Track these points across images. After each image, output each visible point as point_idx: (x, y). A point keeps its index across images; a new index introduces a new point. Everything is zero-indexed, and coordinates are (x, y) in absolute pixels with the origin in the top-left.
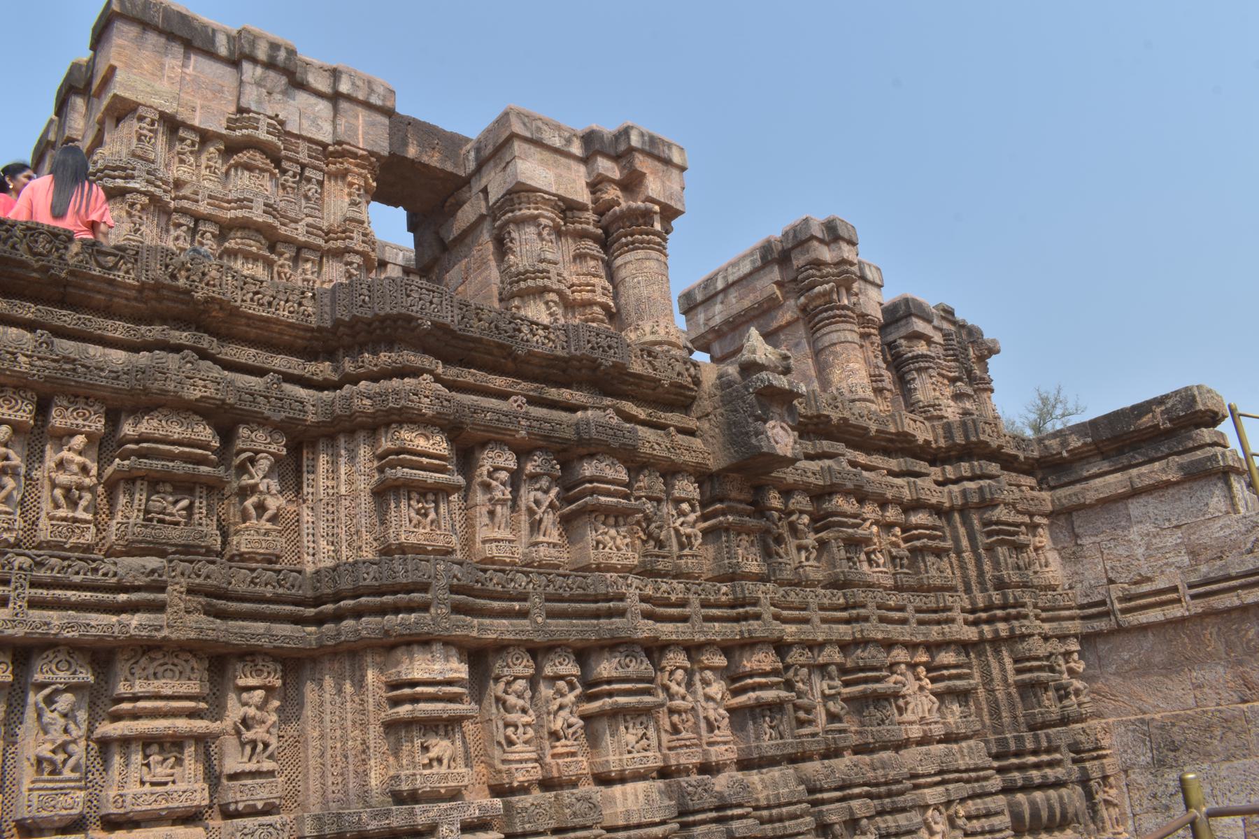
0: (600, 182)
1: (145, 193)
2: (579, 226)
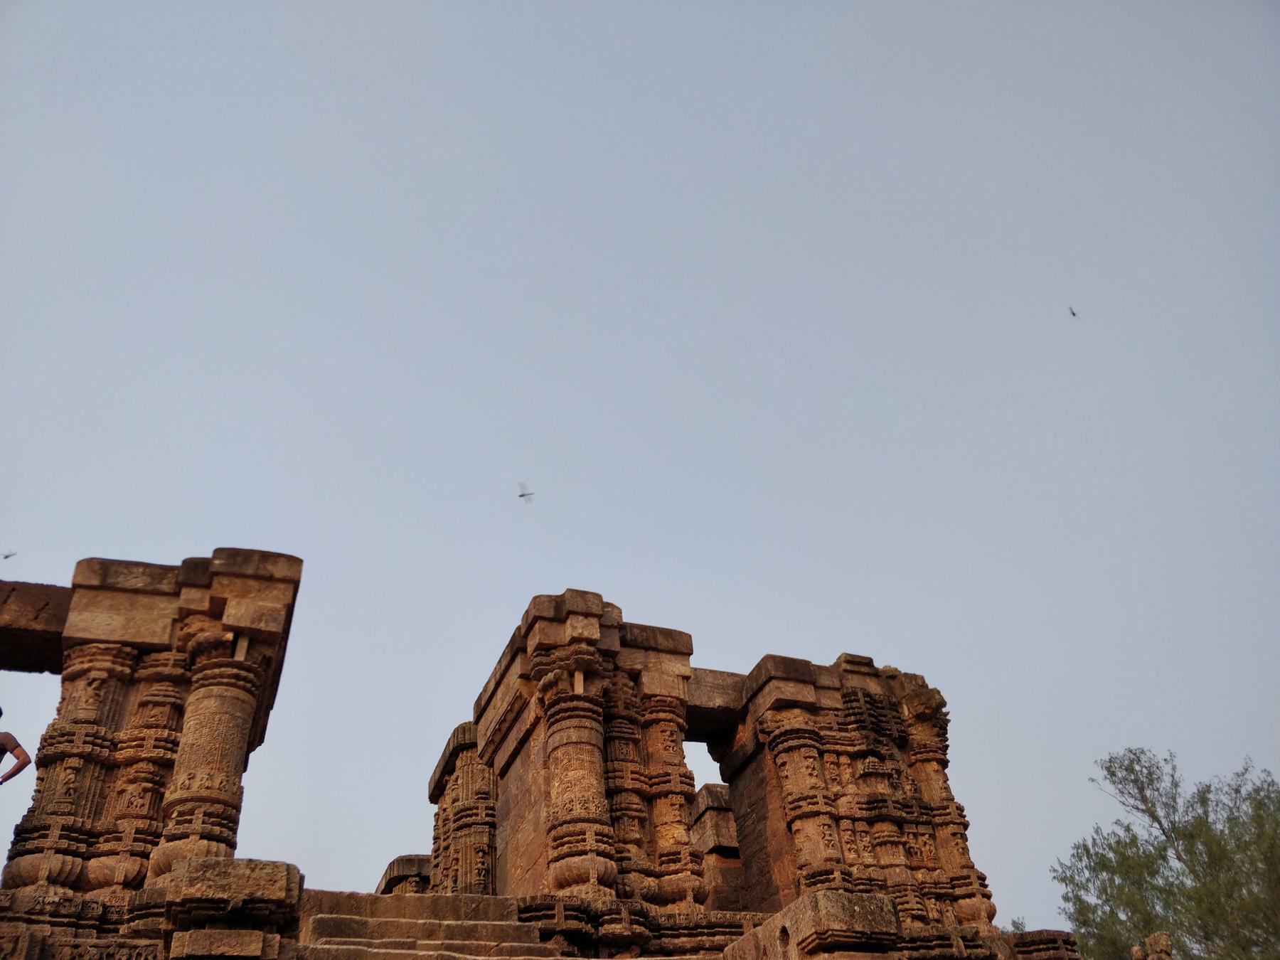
0: (187, 616)
2: (151, 671)
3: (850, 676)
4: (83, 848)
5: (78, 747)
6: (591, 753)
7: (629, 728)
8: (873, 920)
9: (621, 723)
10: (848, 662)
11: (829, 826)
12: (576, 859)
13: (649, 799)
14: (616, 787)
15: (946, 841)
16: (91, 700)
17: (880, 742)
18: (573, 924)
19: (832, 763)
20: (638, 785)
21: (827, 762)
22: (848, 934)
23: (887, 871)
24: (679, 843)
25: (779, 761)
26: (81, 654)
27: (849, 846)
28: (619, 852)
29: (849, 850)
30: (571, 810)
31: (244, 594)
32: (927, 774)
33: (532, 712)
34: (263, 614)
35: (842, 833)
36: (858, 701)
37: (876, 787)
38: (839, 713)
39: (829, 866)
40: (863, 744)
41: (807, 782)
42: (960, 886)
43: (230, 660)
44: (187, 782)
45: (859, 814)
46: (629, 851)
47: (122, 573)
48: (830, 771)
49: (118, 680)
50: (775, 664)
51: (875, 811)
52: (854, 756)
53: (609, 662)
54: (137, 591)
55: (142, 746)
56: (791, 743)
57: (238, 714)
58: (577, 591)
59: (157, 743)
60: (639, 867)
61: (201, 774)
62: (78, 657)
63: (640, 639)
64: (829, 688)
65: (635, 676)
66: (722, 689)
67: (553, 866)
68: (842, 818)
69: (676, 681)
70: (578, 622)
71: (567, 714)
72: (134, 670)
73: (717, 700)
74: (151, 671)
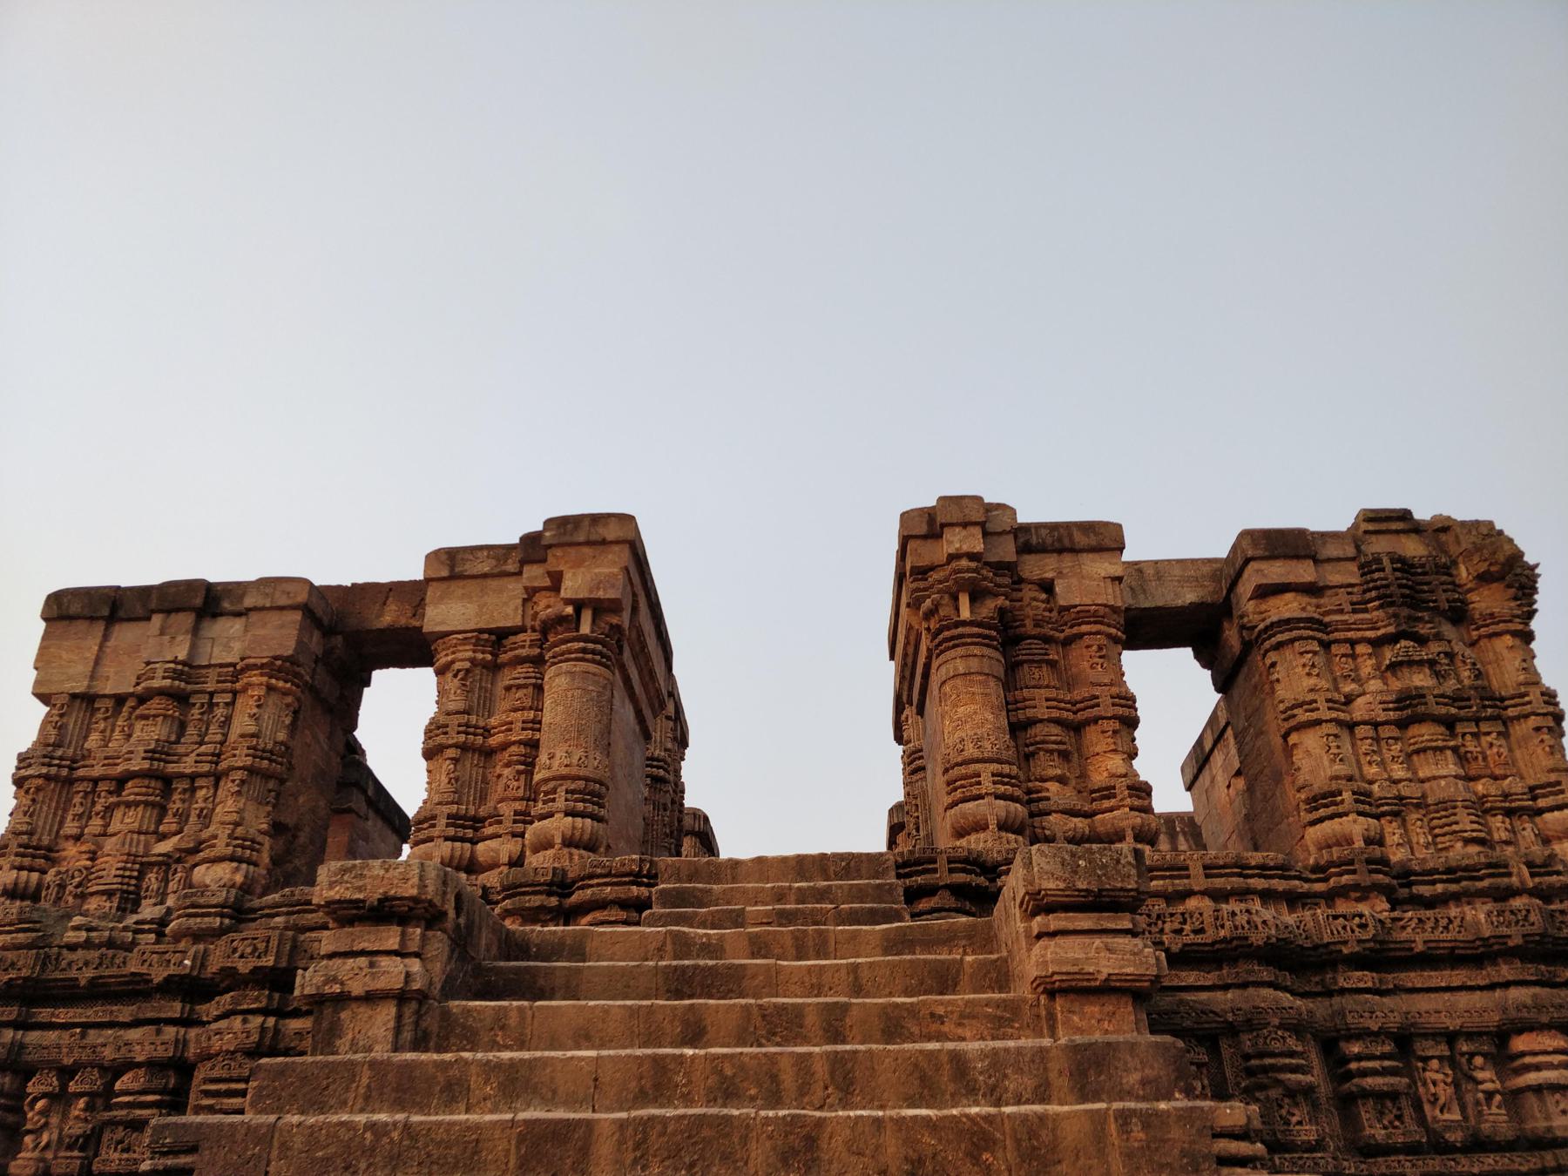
1: (39, 776)
2: (511, 654)
3: (1373, 538)
4: (470, 833)
5: (453, 738)
6: (985, 684)
7: (1042, 649)
8: (1105, 875)
9: (1030, 644)
10: (1369, 520)
11: (1336, 736)
12: (971, 805)
13: (1077, 728)
14: (1028, 718)
15: (1525, 739)
16: (459, 691)
17: (1420, 619)
18: (960, 878)
19: (1343, 656)
20: (1055, 714)
21: (1336, 655)
22: (1066, 893)
23: (1427, 785)
24: (1113, 776)
25: (1268, 662)
26: (444, 646)
27: (1368, 758)
28: (1029, 792)
29: (1370, 763)
30: (962, 751)
31: (578, 564)
32: (1495, 653)
34: (600, 582)
35: (1359, 742)
36: (1383, 570)
38: (1355, 590)
39: (1334, 786)
40: (1390, 625)
41: (1305, 684)
42: (1544, 796)
43: (575, 634)
44: (548, 761)
45: (1382, 717)
46: (1048, 790)
47: (467, 560)
48: (1342, 666)
49: (484, 667)
50: (1253, 540)
51: (1409, 712)
52: (1377, 643)
53: (1003, 575)
54: (485, 576)
55: (510, 730)
56: (1280, 638)
57: (591, 688)
58: (951, 498)
59: (525, 725)
60: (1061, 808)
61: (560, 753)
62: (443, 650)
63: (1049, 540)
64: (1339, 560)
65: (1047, 587)
66: (1196, 581)
67: (948, 813)
68: (1357, 724)
69: (1102, 584)
70: (954, 535)
71: (951, 644)
72: (495, 655)
73: (1188, 596)
74: (511, 654)
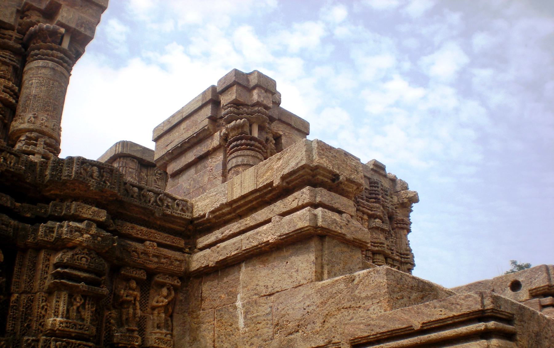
33: (216, 141)
36: (378, 187)
37: (379, 235)
